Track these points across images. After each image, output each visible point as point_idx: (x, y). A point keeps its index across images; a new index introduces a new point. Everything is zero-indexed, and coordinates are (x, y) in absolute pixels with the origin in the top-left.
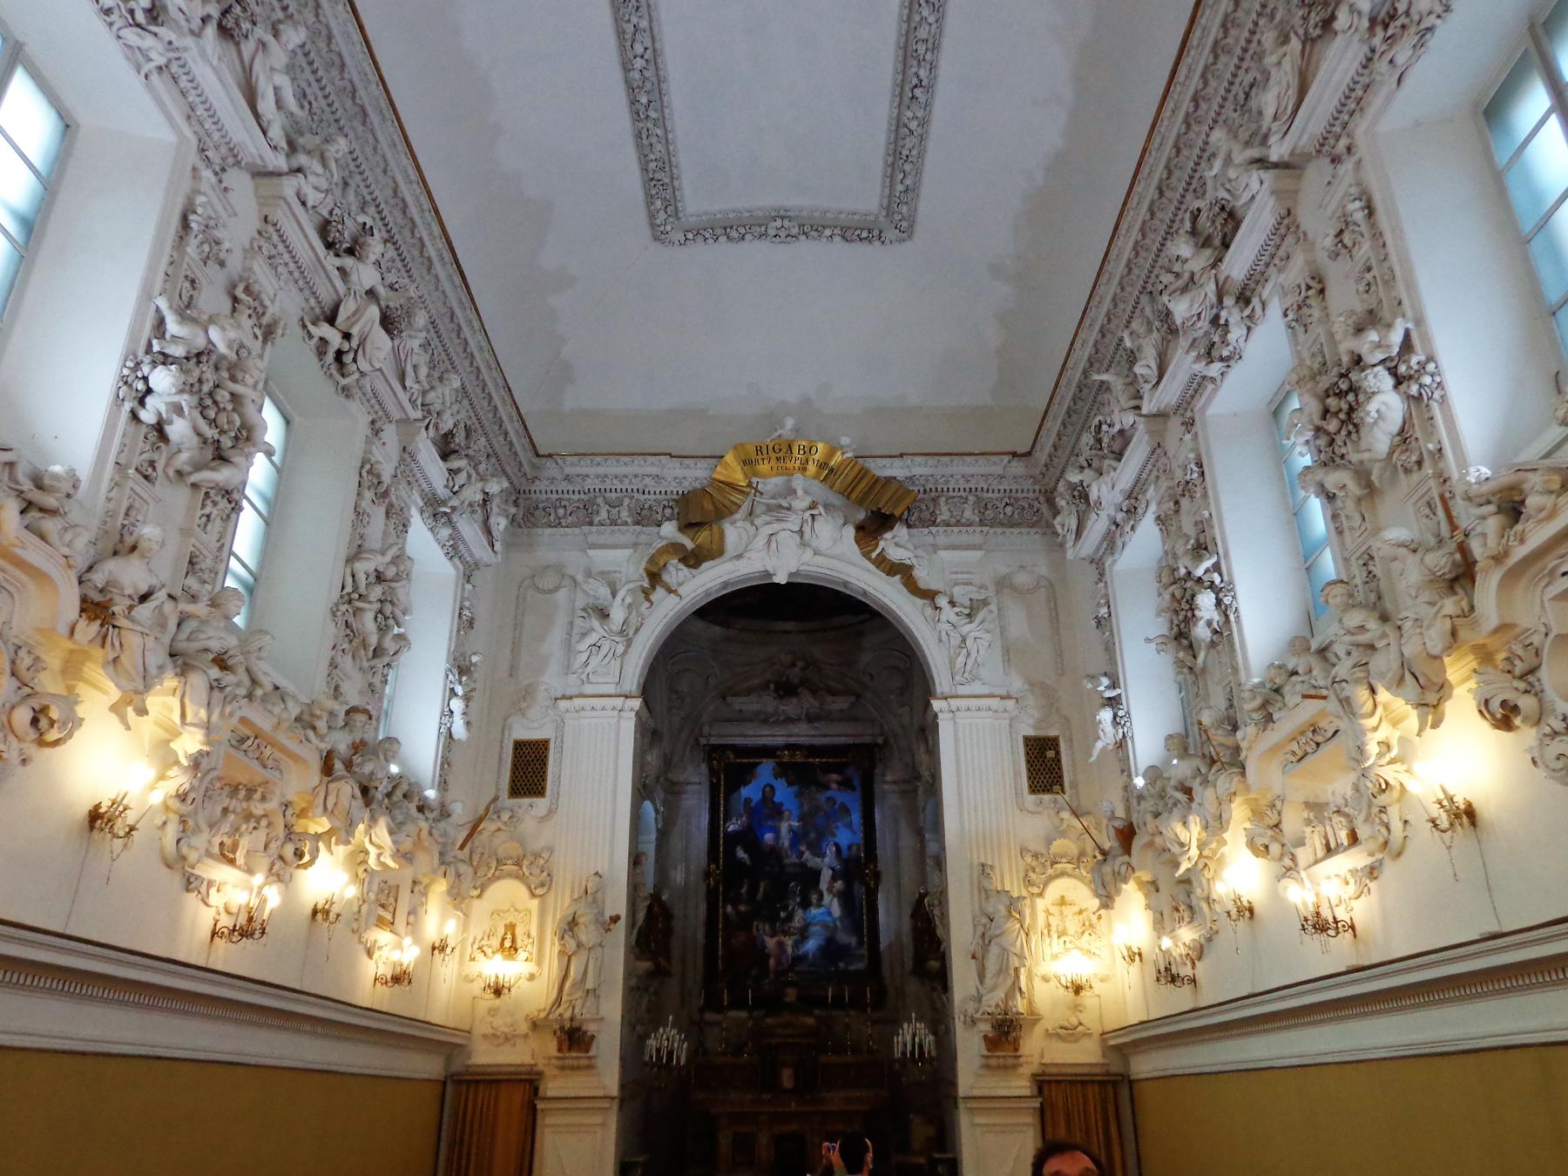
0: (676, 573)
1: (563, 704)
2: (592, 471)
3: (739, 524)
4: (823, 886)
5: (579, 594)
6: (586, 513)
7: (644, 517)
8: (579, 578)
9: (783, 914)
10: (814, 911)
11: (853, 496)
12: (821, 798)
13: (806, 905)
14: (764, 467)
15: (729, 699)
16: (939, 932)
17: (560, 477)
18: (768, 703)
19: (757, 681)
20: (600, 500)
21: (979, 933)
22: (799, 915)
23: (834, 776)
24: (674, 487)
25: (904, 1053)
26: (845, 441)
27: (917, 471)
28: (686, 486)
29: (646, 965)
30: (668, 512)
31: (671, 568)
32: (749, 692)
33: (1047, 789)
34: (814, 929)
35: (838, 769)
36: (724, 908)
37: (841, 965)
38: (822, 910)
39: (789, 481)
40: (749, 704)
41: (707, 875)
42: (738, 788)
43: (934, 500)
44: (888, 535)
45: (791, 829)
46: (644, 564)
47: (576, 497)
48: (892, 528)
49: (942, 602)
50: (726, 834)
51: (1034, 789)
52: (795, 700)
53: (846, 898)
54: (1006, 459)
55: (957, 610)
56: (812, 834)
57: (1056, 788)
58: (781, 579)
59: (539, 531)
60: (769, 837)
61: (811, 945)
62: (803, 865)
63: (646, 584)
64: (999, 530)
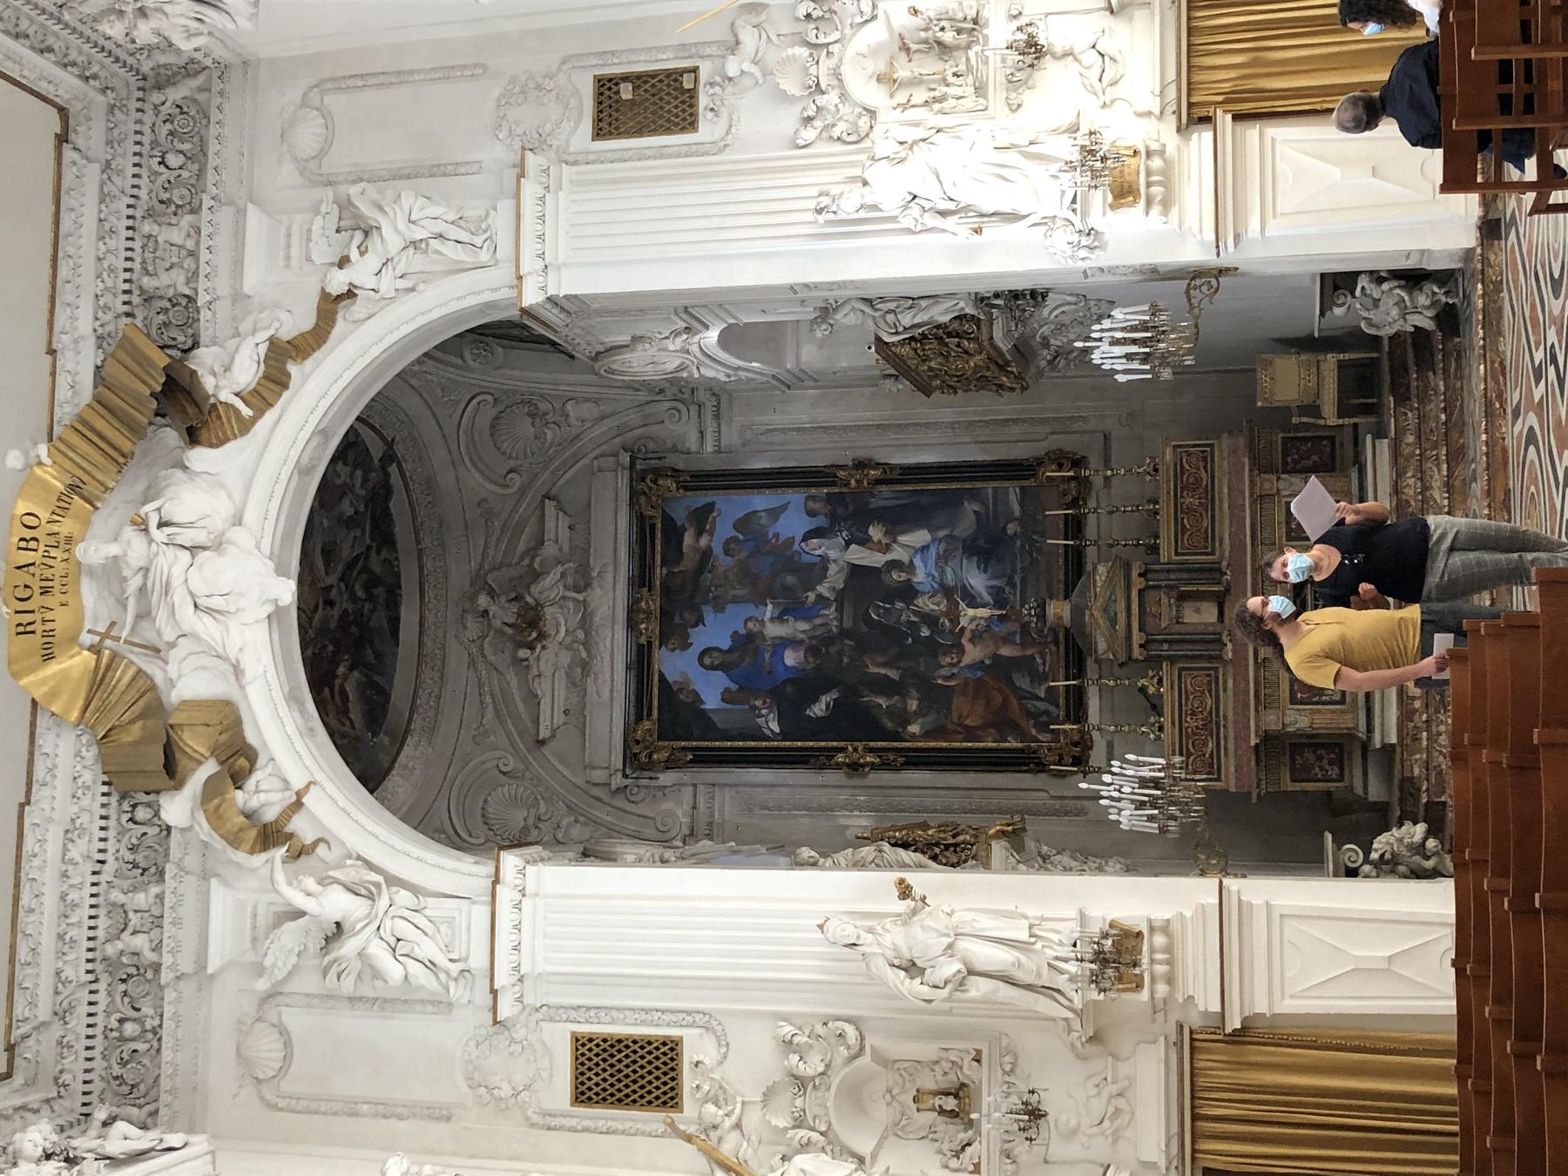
0: (262, 795)
1: (506, 1009)
2: (47, 963)
3: (173, 674)
4: (876, 559)
5: (294, 986)
6: (135, 977)
7: (148, 863)
8: (262, 985)
9: (925, 632)
10: (920, 577)
11: (126, 446)
12: (723, 562)
13: (908, 592)
14: (61, 620)
15: (544, 734)
16: (941, 314)
17: (57, 1031)
18: (551, 660)
19: (514, 683)
20: (110, 950)
21: (938, 222)
22: (926, 604)
23: (688, 539)
24: (93, 802)
25: (1145, 358)
26: (14, 460)
27: (85, 325)
28: (91, 776)
29: (999, 849)
30: (142, 814)
31: (254, 803)
32: (533, 699)
33: (692, 94)
34: (950, 579)
35: (673, 534)
36: (914, 737)
37: (1012, 528)
38: (917, 562)
39: (92, 572)
40: (553, 698)
41: (855, 768)
42: (703, 715)
43: (148, 299)
44: (209, 383)
45: (779, 618)
46: (241, 857)
47: (102, 998)
48: (193, 373)
49: (338, 282)
50: (785, 736)
51: (690, 124)
52: (549, 612)
53: (897, 520)
54: (69, 154)
55: (354, 254)
56: (784, 580)
57: (687, 84)
58: (286, 591)
59: (166, 1070)
60: (791, 658)
61: (978, 581)
62: (841, 596)
63: (280, 852)
64: (211, 177)
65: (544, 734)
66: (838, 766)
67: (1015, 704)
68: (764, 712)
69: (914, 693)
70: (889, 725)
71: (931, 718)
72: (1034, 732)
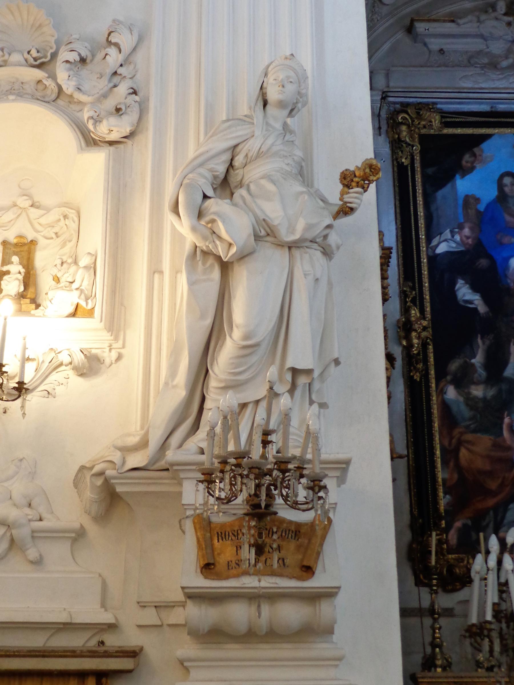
36: (441, 392)
50: (433, 259)
65: (420, 27)
66: (405, 310)
67: (491, 502)
68: (457, 238)
69: (491, 393)
70: (454, 366)
71: (462, 410)
72: (458, 524)
